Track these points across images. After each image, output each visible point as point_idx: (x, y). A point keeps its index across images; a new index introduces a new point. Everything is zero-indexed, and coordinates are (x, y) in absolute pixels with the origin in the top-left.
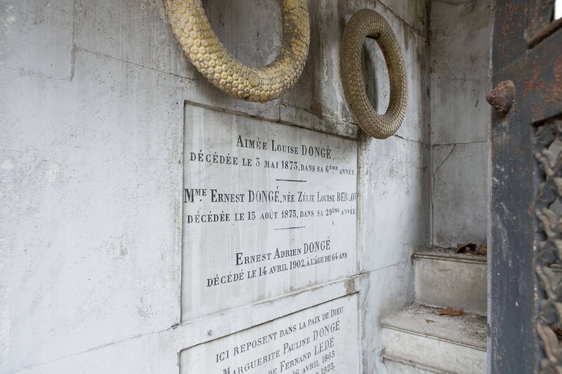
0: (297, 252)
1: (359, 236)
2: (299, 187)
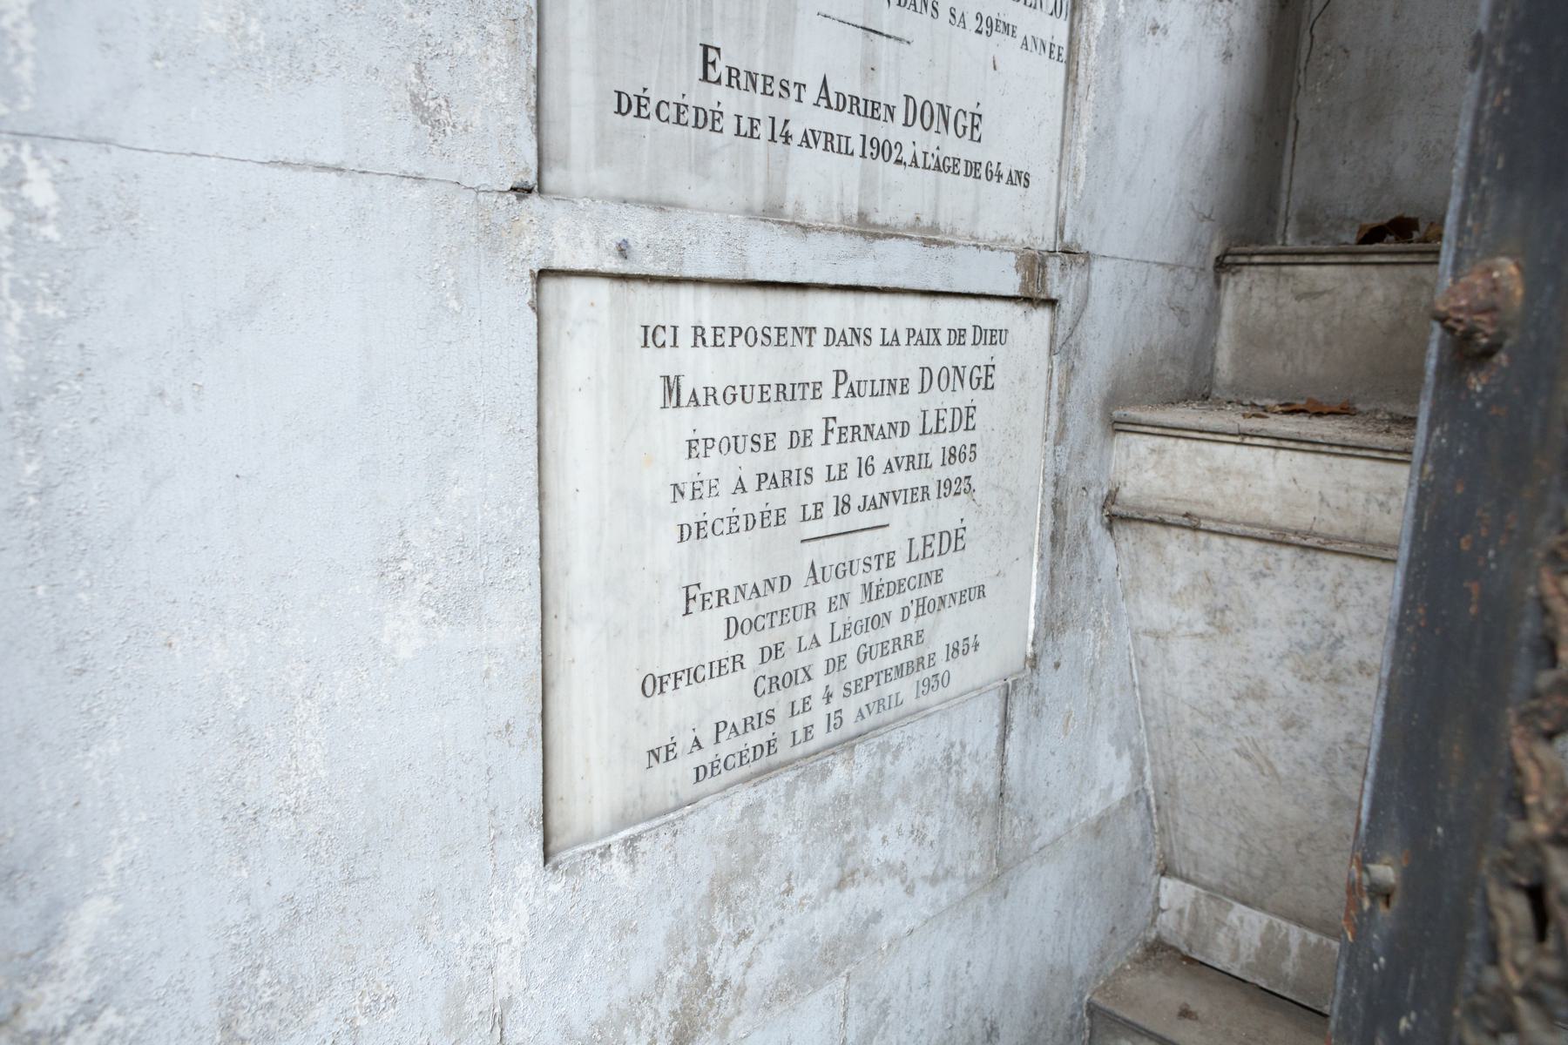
0: (882, 111)
1: (1068, 134)
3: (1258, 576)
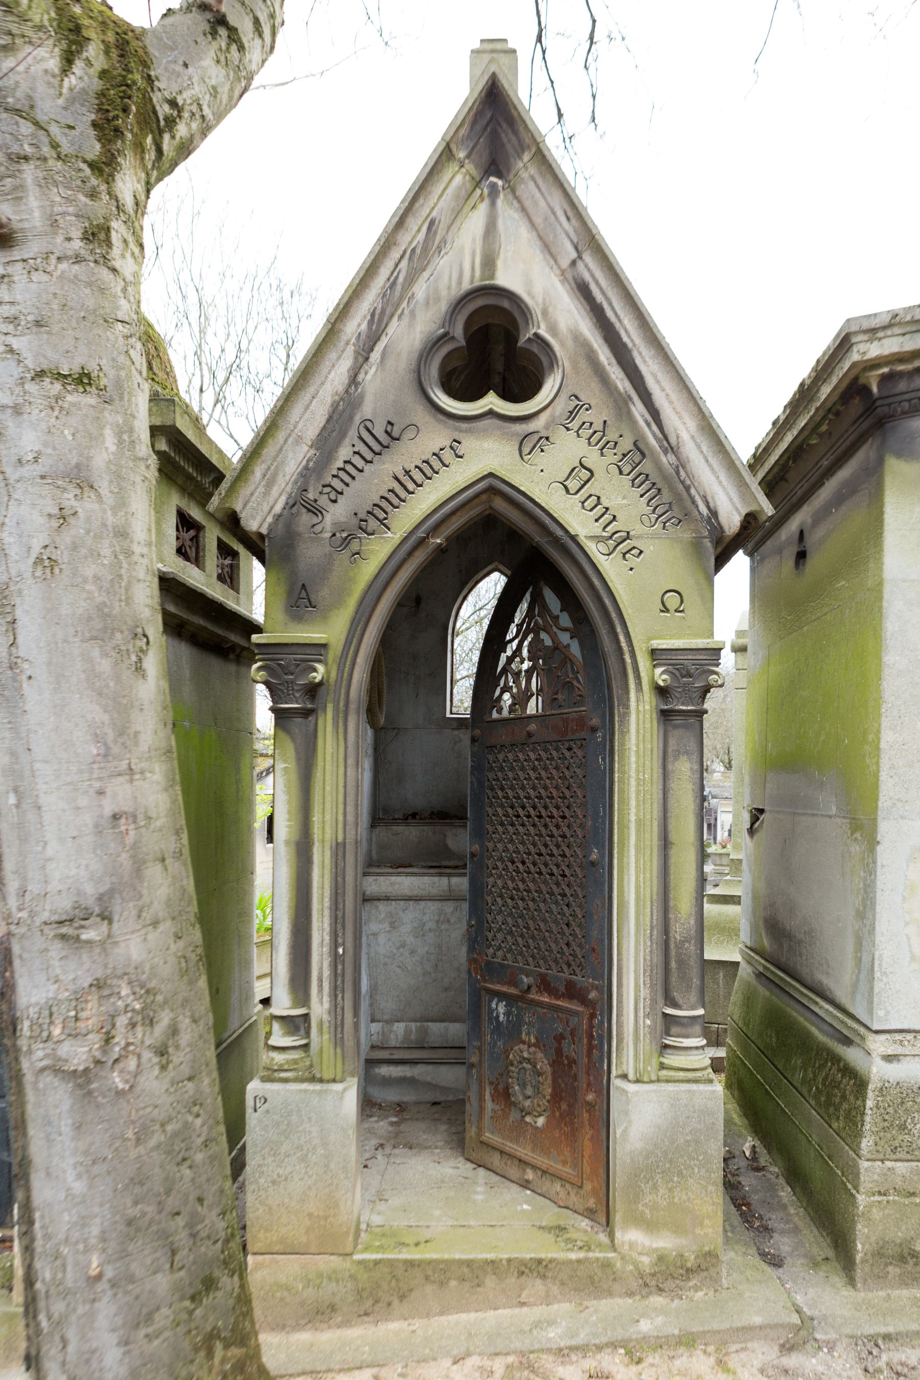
3: (404, 911)
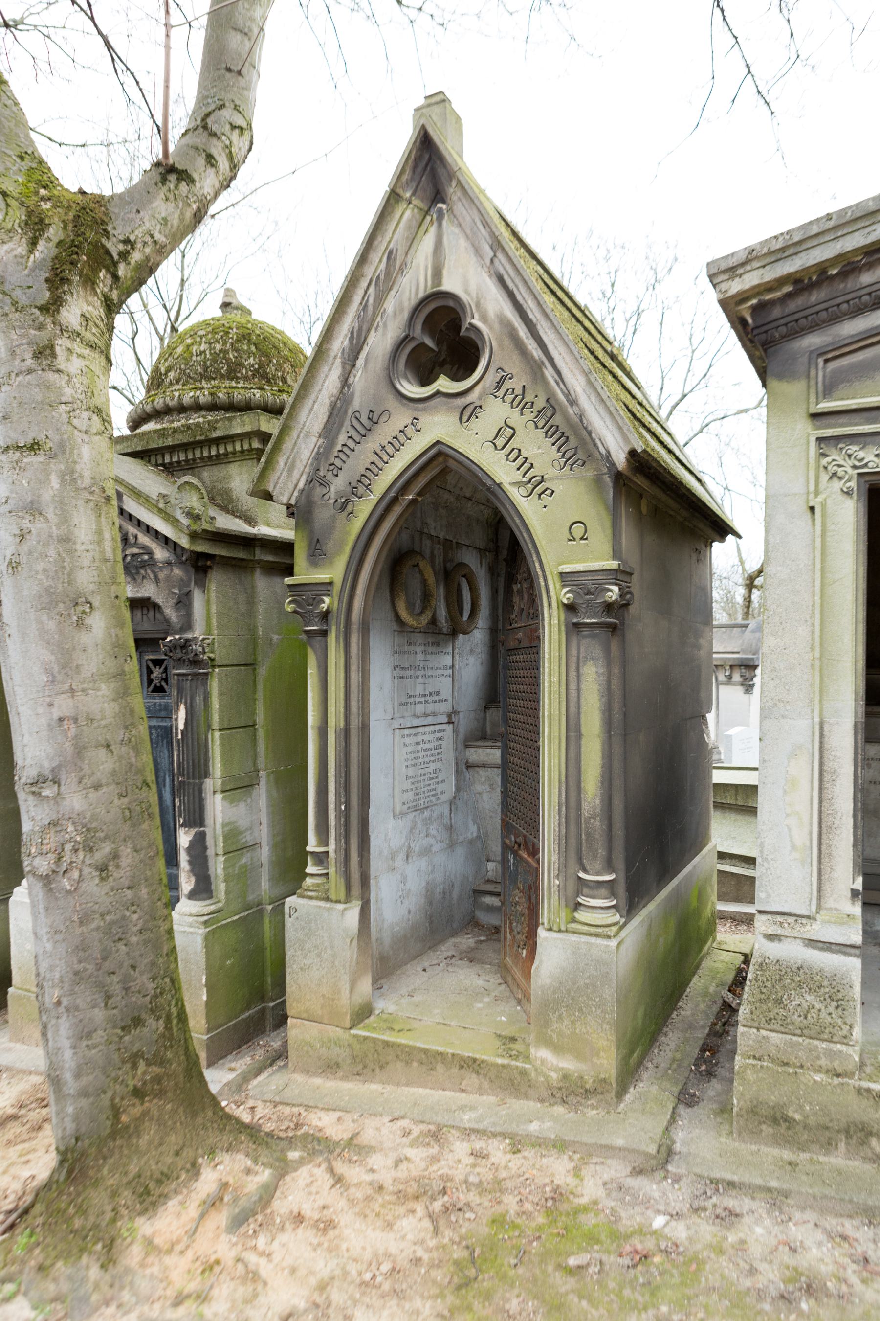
2: (427, 663)
